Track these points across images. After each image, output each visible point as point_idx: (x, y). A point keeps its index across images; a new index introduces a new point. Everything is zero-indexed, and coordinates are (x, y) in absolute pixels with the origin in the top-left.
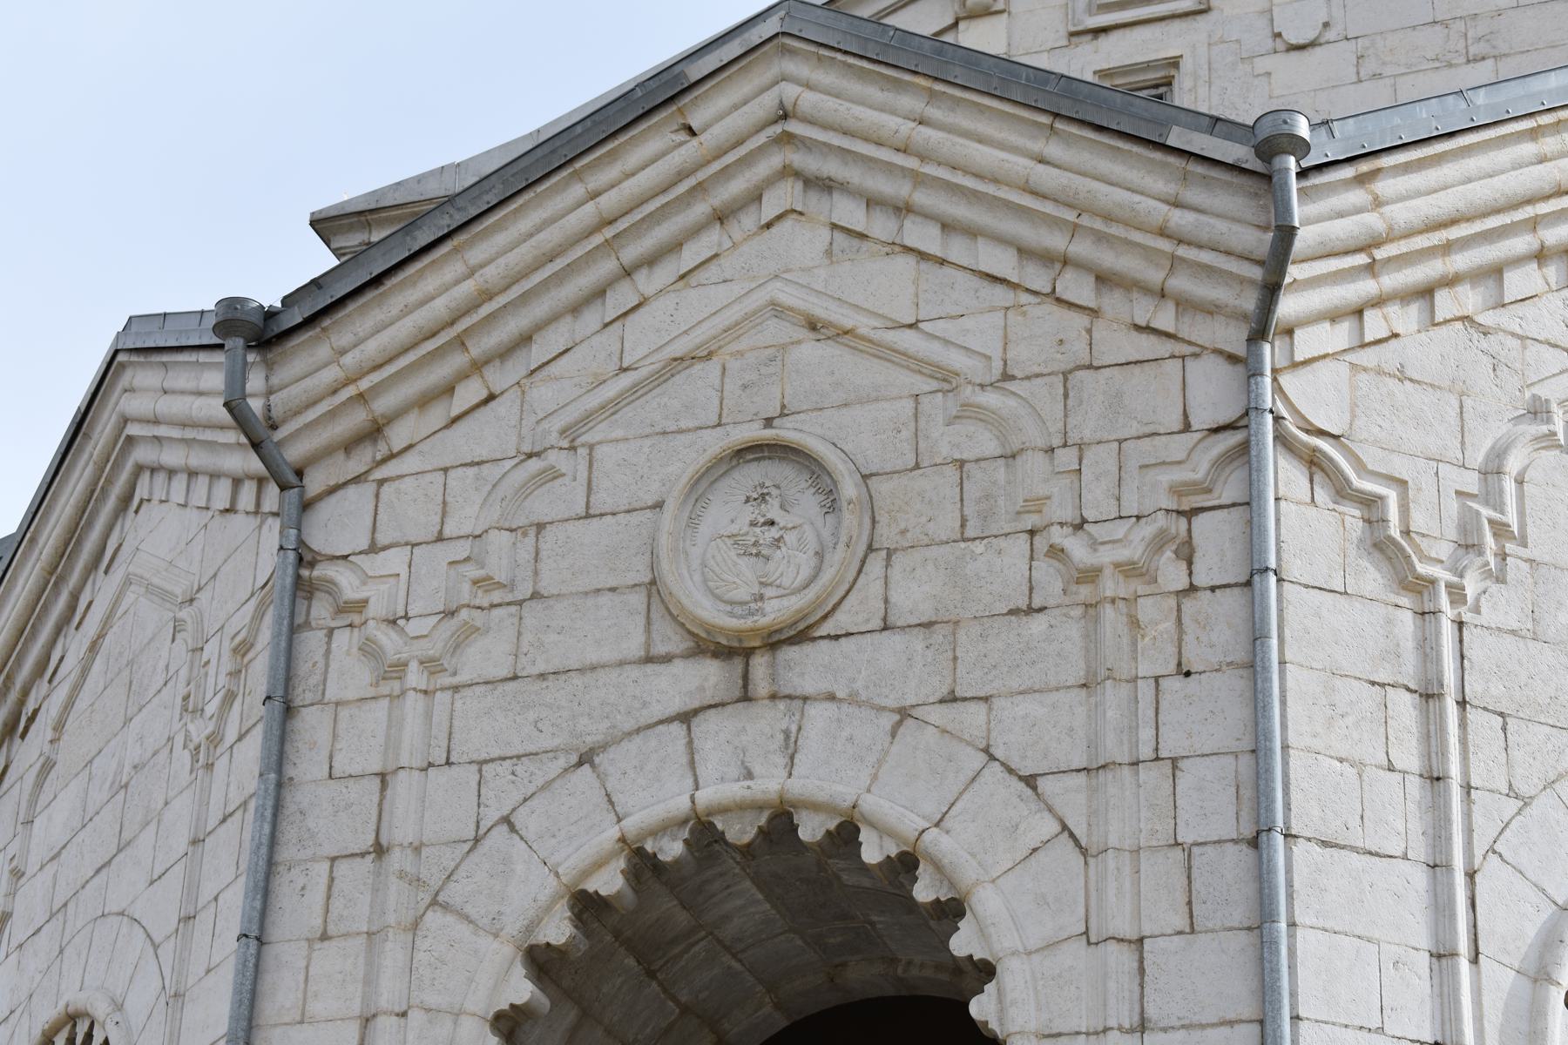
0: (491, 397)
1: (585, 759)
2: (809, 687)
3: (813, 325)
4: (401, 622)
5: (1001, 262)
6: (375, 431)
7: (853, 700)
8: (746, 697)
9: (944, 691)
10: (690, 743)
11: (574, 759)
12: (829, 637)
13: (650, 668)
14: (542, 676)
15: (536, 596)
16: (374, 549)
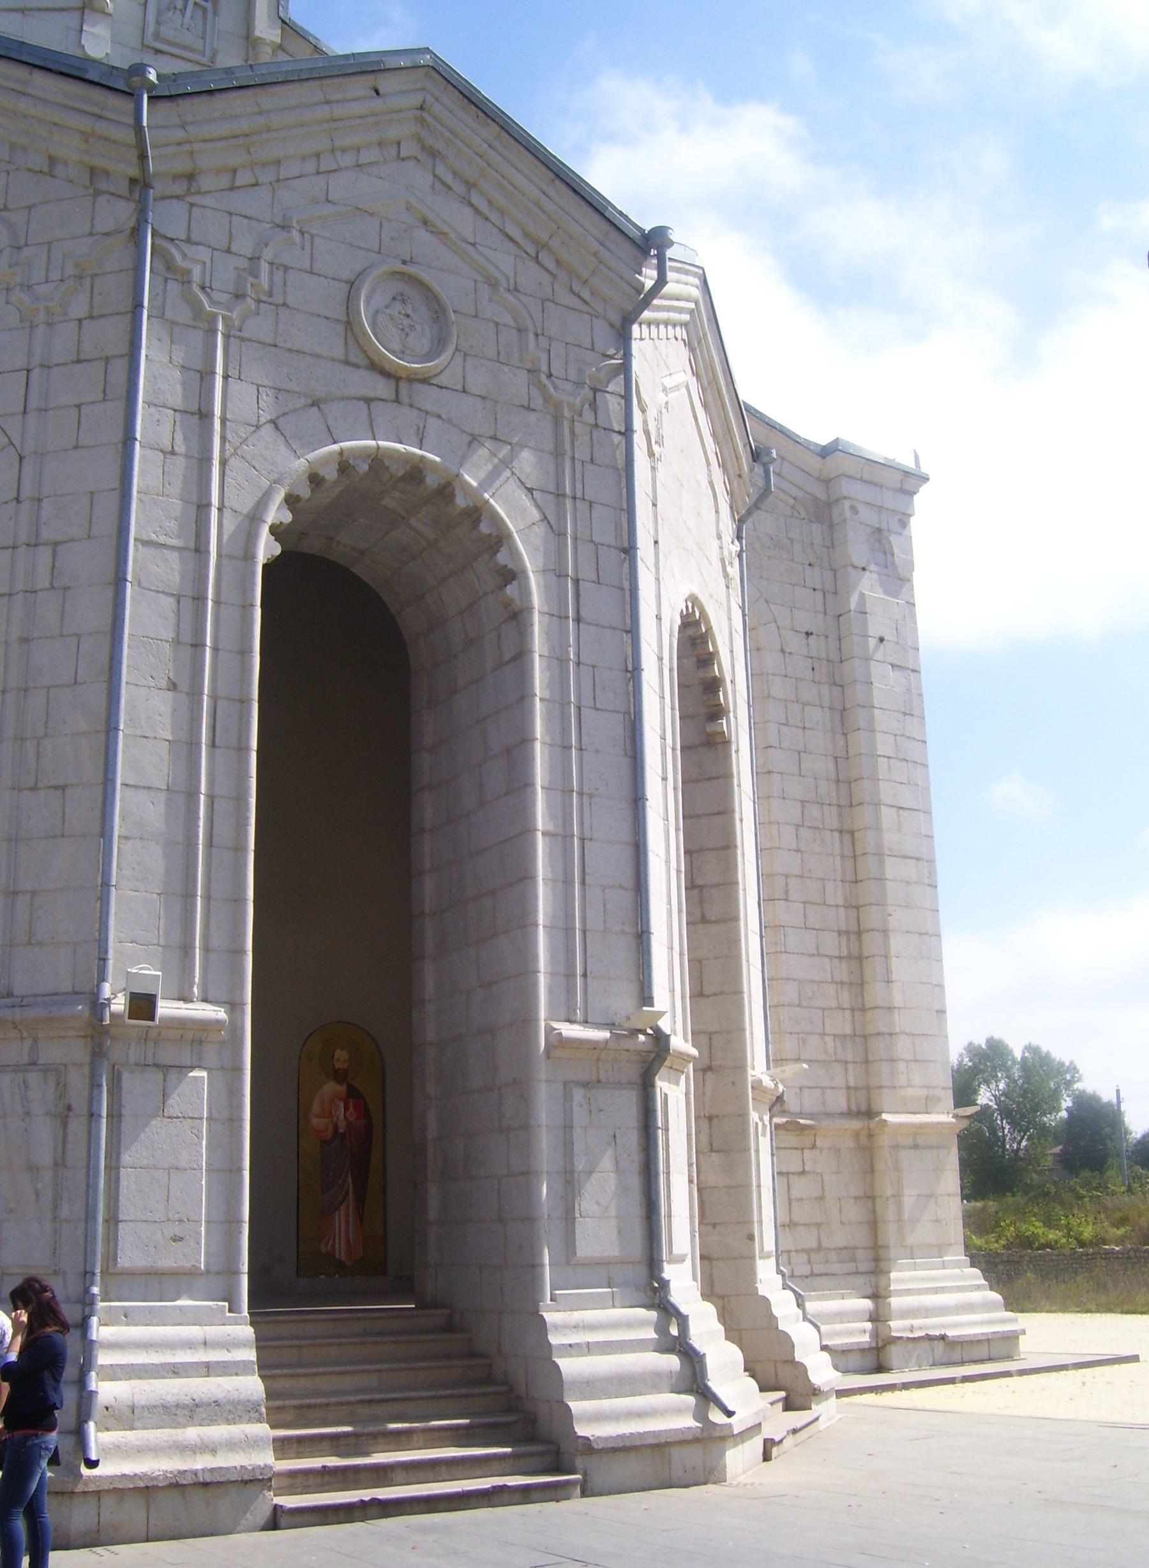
0: (256, 185)
1: (315, 404)
2: (428, 407)
3: (425, 222)
4: (208, 290)
5: (515, 233)
6: (190, 177)
7: (449, 421)
8: (397, 401)
9: (492, 433)
10: (370, 414)
11: (310, 401)
12: (437, 386)
13: (347, 368)
14: (290, 350)
15: (284, 304)
16: (188, 241)
